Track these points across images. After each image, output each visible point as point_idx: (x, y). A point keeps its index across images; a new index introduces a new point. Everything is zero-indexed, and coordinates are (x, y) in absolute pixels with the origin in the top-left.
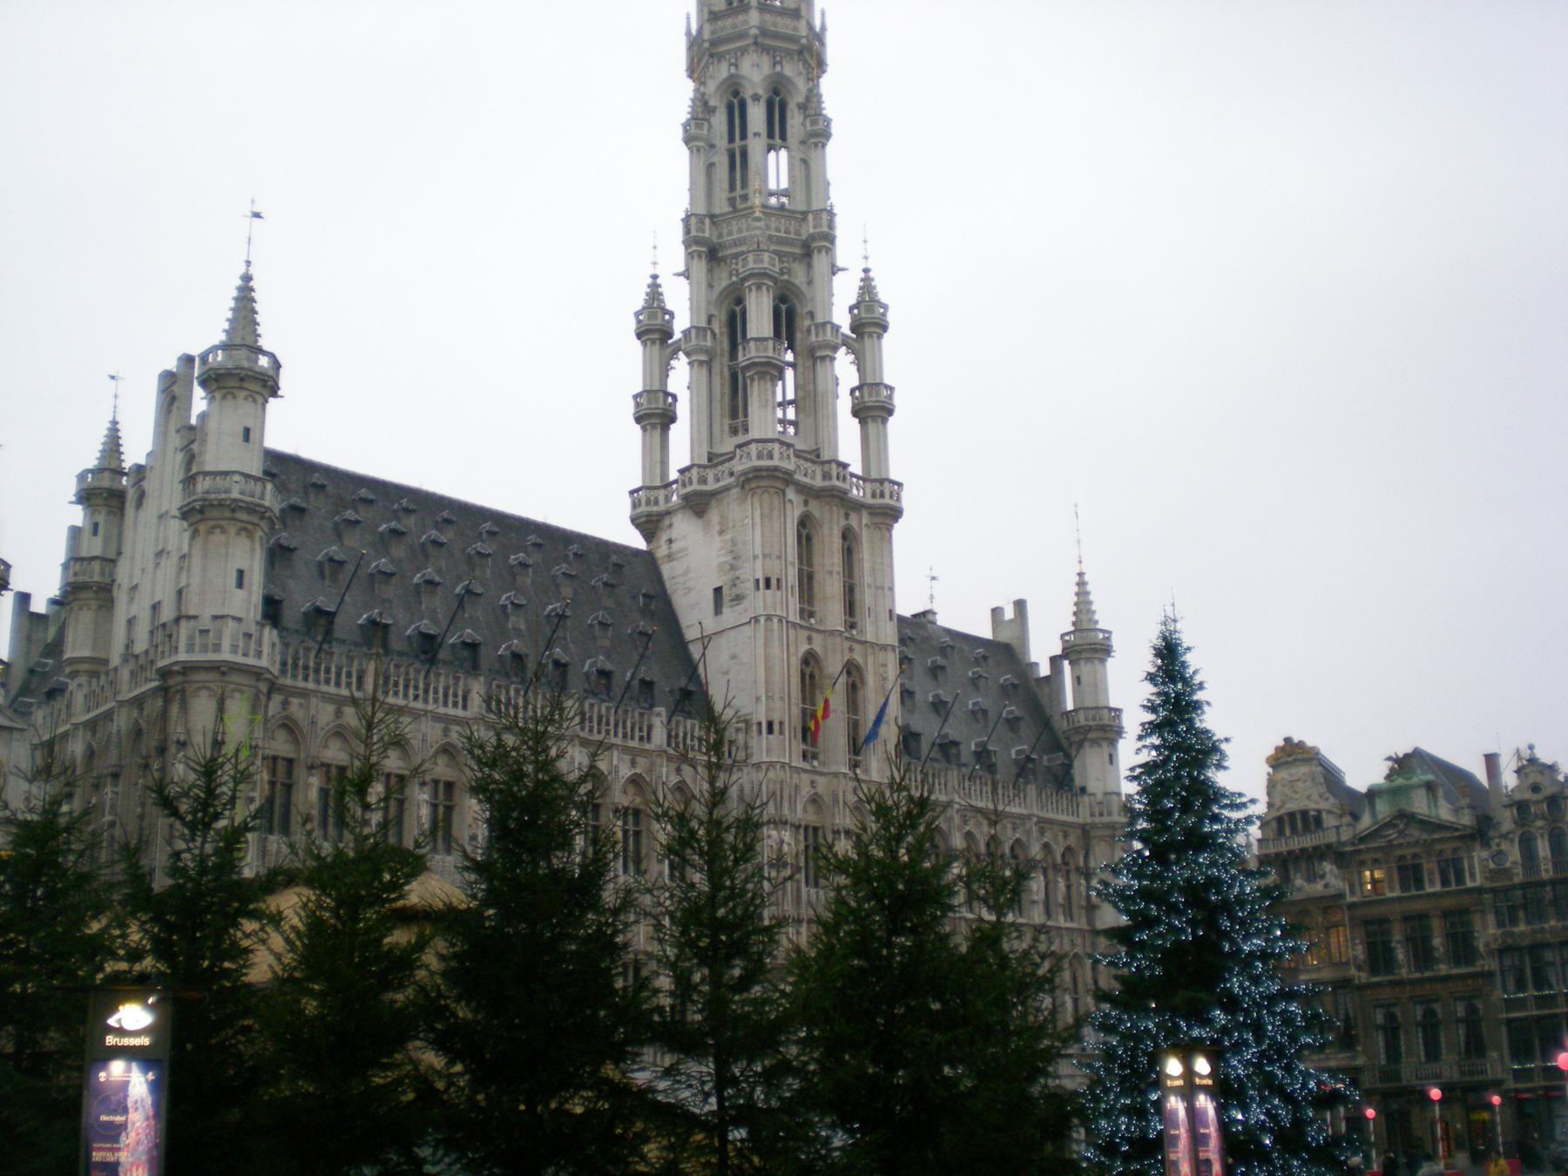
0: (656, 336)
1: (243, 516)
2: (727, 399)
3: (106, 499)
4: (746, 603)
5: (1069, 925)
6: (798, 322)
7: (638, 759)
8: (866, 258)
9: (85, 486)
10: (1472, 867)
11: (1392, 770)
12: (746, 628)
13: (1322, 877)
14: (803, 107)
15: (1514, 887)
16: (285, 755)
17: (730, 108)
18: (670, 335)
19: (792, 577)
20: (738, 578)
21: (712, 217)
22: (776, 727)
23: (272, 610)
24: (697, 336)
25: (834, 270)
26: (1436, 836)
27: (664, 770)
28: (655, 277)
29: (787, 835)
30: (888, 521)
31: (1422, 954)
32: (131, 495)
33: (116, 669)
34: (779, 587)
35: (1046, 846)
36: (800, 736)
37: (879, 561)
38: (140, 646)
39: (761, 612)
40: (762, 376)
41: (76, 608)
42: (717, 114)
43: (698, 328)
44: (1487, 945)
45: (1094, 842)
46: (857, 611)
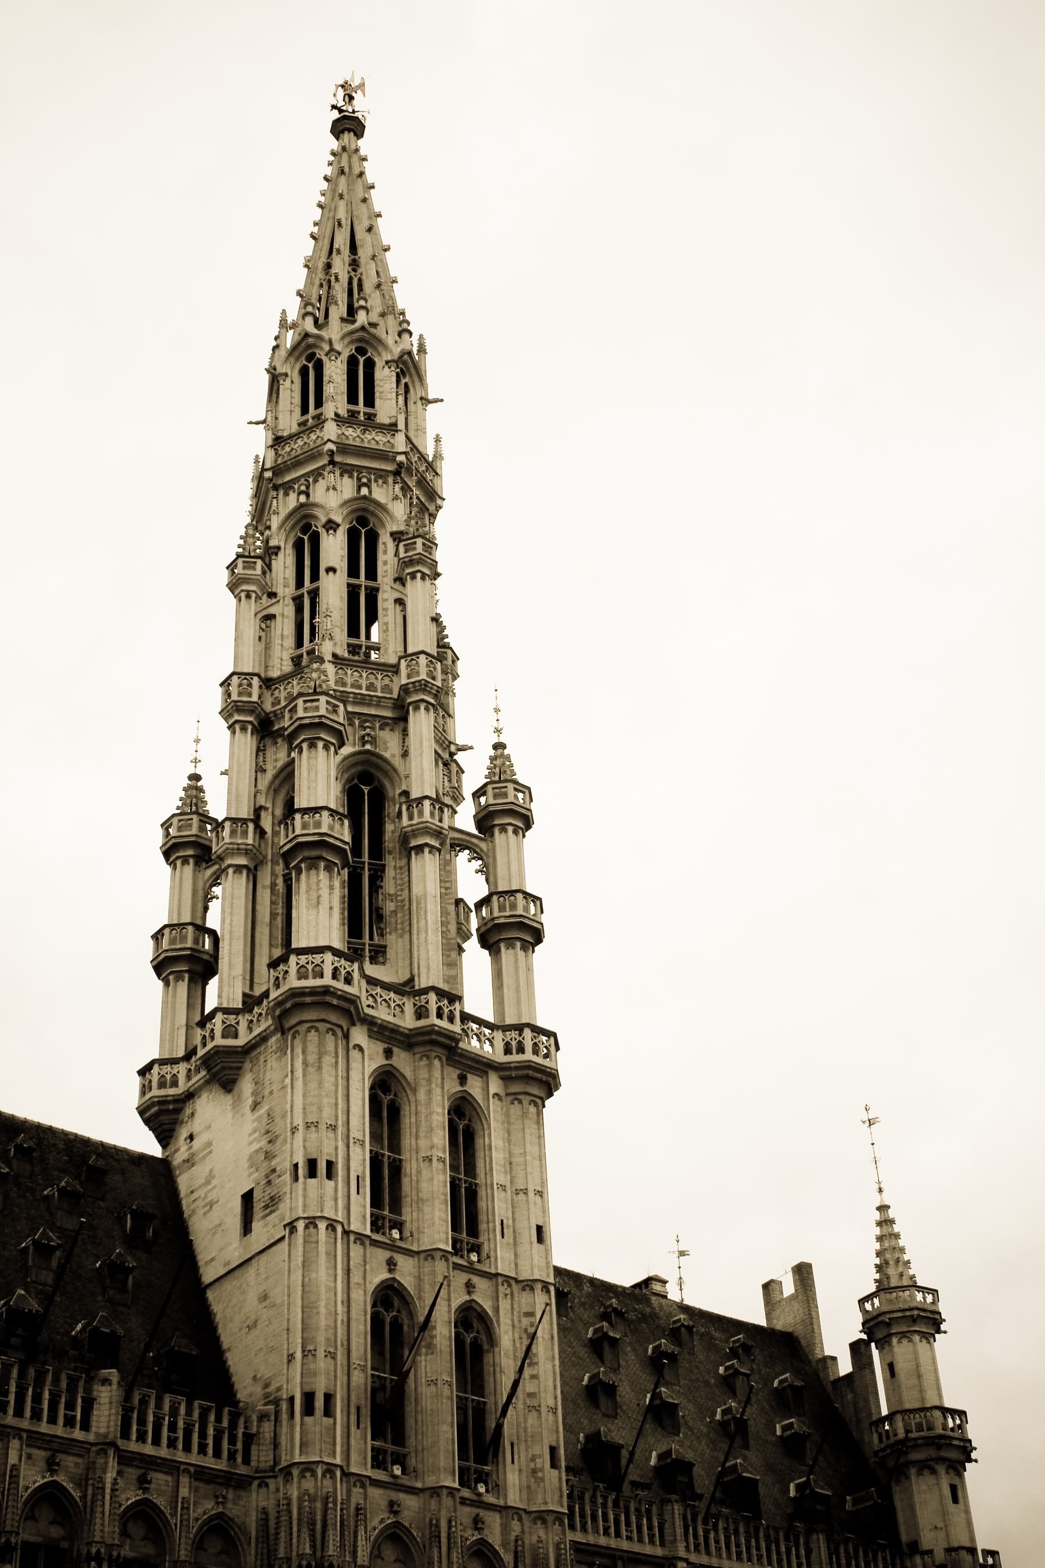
0: (190, 852)
6: (391, 809)
8: (498, 731)
12: (284, 1245)
17: (298, 546)
20: (274, 1171)
22: (319, 1403)
24: (233, 833)
27: (110, 1476)
28: (195, 777)
30: (535, 1090)
34: (330, 1174)
37: (517, 1150)
40: (313, 864)
42: (281, 555)
43: (234, 820)
46: (483, 1227)
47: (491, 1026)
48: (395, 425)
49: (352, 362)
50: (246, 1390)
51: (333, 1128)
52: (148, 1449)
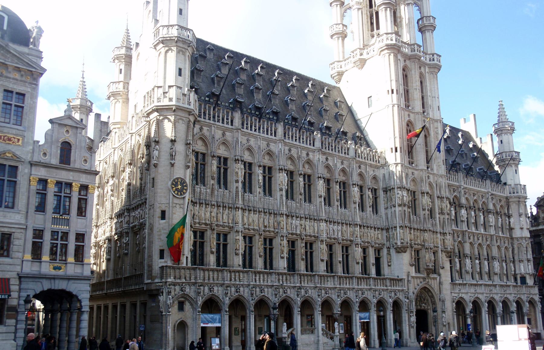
7: (344, 162)
16: (201, 151)
19: (402, 91)
29: (405, 193)
30: (436, 70)
35: (494, 205)
45: (511, 204)
46: (425, 106)
47: (426, 54)
51: (396, 81)
52: (360, 160)
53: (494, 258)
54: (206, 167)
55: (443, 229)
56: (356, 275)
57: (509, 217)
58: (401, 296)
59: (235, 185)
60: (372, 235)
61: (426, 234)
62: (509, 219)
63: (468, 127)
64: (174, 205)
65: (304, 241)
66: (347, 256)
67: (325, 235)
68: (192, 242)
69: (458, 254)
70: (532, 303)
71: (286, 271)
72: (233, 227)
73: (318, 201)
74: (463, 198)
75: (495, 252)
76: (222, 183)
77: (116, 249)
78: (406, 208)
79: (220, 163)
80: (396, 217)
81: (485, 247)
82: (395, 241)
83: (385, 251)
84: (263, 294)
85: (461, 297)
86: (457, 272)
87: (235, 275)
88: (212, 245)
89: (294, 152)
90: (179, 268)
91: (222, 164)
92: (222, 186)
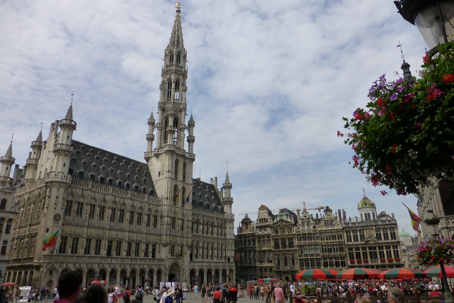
0: (152, 124)
1: (66, 153)
2: (164, 136)
3: (38, 147)
4: (165, 175)
5: (221, 237)
7: (142, 203)
9: (33, 144)
10: (293, 230)
11: (280, 211)
12: (164, 179)
13: (267, 230)
14: (182, 85)
15: (301, 234)
18: (154, 124)
21: (164, 103)
23: (71, 171)
24: (159, 125)
25: (186, 114)
26: (287, 224)
27: (147, 206)
29: (169, 220)
31: (284, 245)
32: (43, 146)
33: (36, 181)
35: (218, 223)
36: (173, 200)
38: (42, 178)
39: (167, 176)
41: (29, 169)
43: (159, 123)
44: (296, 244)
45: (227, 222)
46: (185, 177)
48: (183, 67)
49: (178, 55)
50: (158, 195)
51: (171, 167)
52: (150, 202)
53: (215, 249)
54: (72, 207)
55: (187, 236)
56: (141, 258)
57: (225, 228)
58: (162, 267)
59: (85, 215)
60: (152, 238)
61: (178, 238)
62: (225, 230)
63: (213, 183)
64: (54, 226)
65: (117, 241)
66: (138, 248)
67: (127, 238)
68: (60, 243)
69: (196, 247)
70: (231, 270)
71: (106, 256)
72: (82, 235)
73: (126, 222)
74: (202, 220)
75: (215, 246)
76: (79, 214)
77: (20, 243)
78: (169, 226)
79: (79, 205)
80: (164, 230)
81: (211, 243)
82: (162, 241)
83: (158, 246)
84: (92, 267)
85: (194, 268)
86: (195, 256)
87: (79, 259)
88: (70, 244)
89: (117, 199)
90: (52, 255)
91: (80, 205)
92: (79, 215)
